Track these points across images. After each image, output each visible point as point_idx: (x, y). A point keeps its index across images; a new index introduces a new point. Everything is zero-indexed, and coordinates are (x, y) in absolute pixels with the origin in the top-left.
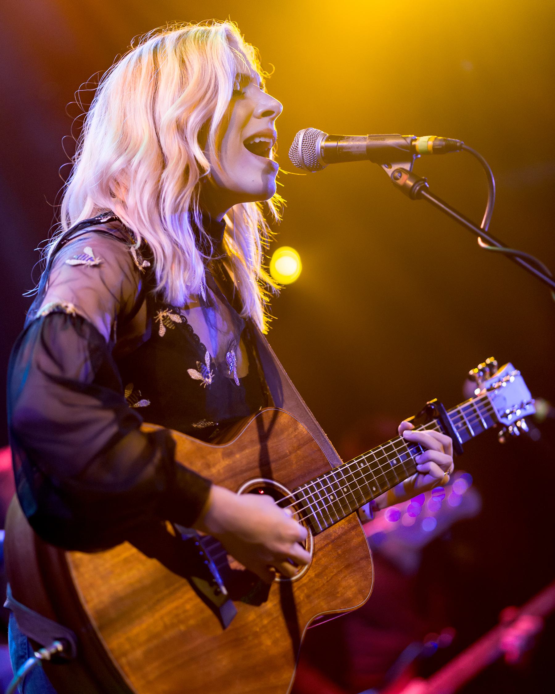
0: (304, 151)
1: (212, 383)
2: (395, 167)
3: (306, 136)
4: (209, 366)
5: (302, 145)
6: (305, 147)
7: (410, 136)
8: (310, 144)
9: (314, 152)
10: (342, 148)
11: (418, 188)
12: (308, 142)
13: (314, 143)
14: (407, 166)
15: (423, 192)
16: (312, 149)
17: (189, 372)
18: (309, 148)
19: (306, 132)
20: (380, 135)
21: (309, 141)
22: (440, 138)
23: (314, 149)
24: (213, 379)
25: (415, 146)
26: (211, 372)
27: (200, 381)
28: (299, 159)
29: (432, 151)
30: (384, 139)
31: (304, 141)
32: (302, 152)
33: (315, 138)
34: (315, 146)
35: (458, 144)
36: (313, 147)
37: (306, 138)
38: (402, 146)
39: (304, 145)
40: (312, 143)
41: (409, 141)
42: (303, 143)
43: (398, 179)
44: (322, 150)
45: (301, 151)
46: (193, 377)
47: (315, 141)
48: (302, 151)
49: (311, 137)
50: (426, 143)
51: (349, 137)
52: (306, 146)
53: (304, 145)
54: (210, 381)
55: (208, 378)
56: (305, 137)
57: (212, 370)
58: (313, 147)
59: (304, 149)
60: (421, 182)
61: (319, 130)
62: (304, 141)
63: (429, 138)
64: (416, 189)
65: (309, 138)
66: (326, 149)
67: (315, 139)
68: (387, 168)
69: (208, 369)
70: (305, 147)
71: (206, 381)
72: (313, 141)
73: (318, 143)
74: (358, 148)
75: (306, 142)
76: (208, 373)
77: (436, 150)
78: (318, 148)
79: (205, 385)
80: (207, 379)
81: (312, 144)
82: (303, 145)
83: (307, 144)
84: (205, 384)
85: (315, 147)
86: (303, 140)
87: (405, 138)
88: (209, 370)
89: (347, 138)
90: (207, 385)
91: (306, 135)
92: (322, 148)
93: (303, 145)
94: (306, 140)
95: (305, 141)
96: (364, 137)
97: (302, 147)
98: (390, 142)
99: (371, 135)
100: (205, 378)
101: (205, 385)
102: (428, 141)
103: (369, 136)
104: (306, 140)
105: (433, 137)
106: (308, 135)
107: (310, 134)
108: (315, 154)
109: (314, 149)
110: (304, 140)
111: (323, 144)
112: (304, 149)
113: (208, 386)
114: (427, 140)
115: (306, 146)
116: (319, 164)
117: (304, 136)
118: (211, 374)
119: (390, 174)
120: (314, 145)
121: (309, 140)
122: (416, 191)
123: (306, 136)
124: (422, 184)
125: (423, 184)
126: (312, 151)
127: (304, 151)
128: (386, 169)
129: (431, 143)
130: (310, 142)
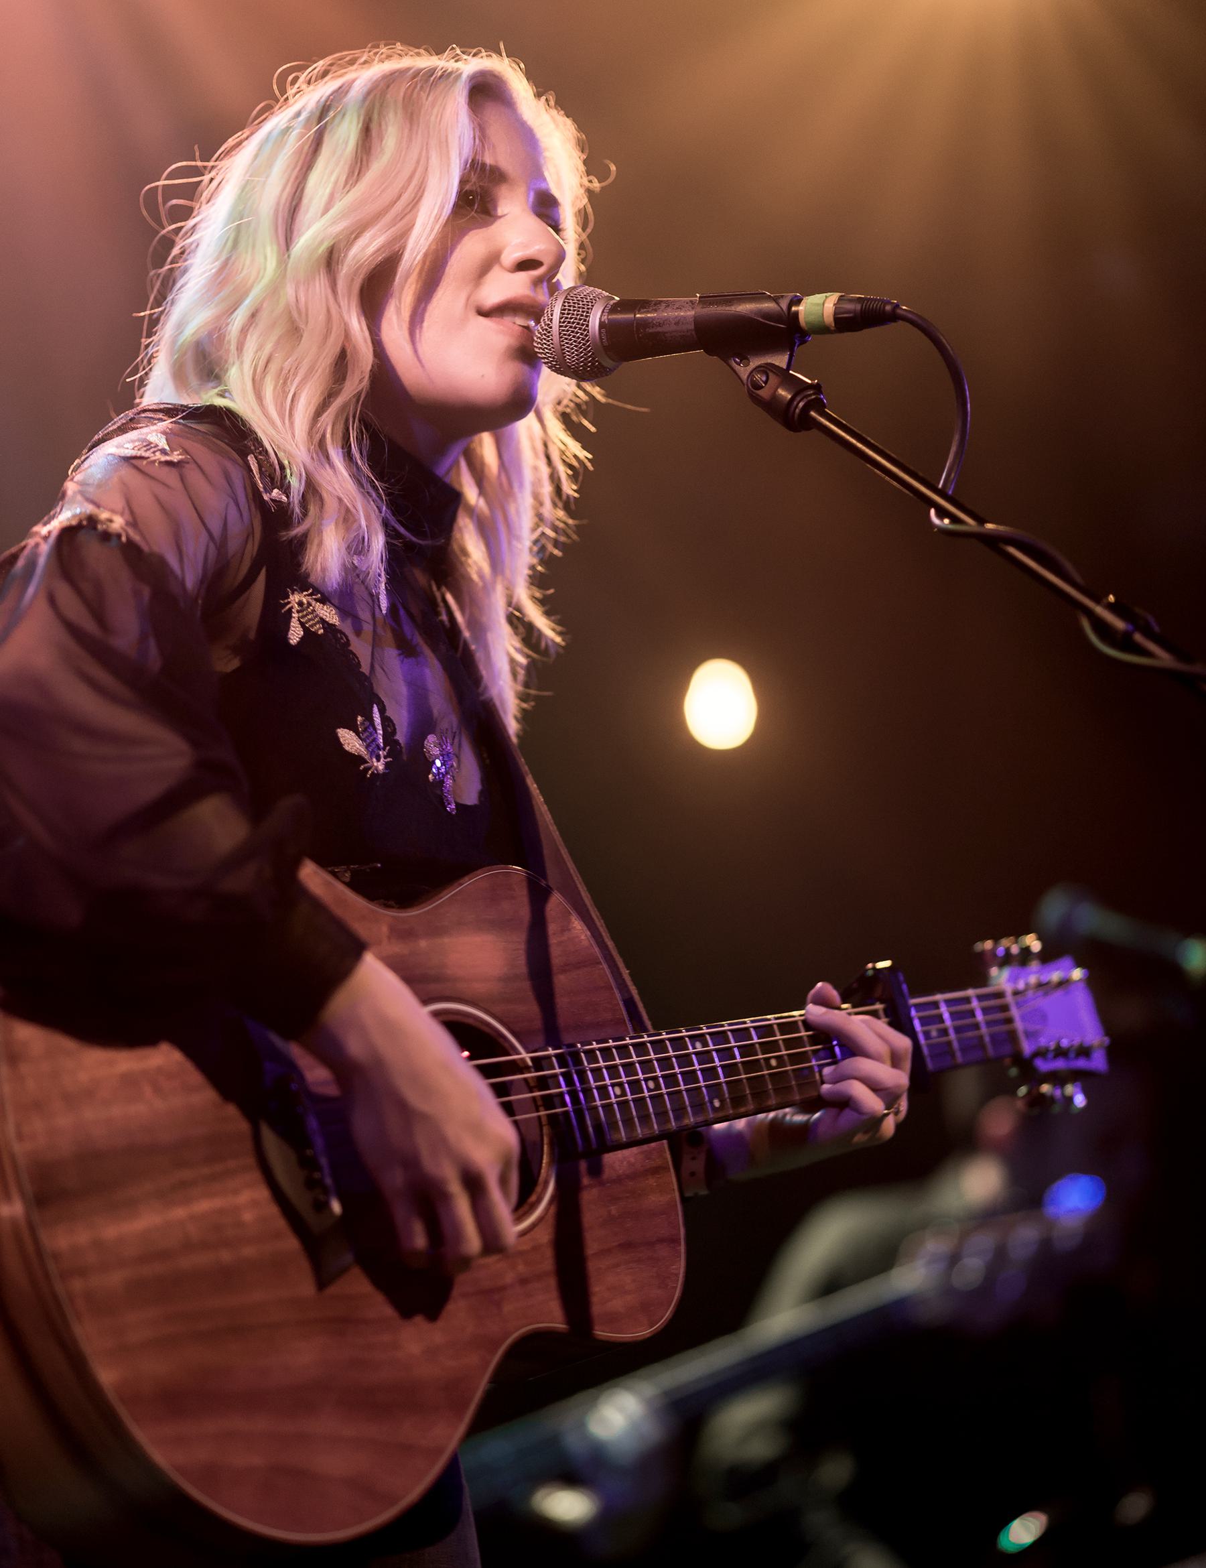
0: (565, 335)
3: (569, 303)
5: (560, 322)
8: (576, 319)
12: (573, 314)
13: (587, 316)
17: (339, 735)
18: (575, 328)
21: (575, 313)
23: (585, 330)
28: (553, 348)
31: (564, 314)
33: (588, 305)
34: (588, 322)
36: (583, 325)
37: (570, 306)
39: (564, 322)
40: (582, 315)
42: (561, 318)
46: (347, 748)
47: (588, 312)
48: (560, 334)
52: (569, 322)
53: (564, 322)
56: (566, 304)
58: (583, 325)
59: (563, 330)
62: (564, 314)
65: (574, 307)
67: (588, 309)
70: (566, 327)
75: (568, 314)
81: (580, 319)
82: (562, 320)
83: (571, 318)
86: (562, 310)
91: (569, 299)
93: (562, 320)
94: (570, 310)
95: (566, 312)
97: (560, 326)
104: (570, 310)
106: (573, 300)
107: (577, 298)
109: (585, 330)
110: (564, 310)
112: (563, 330)
115: (569, 322)
116: (597, 361)
121: (574, 311)
123: (569, 303)
126: (582, 334)
127: (565, 335)
130: (577, 315)
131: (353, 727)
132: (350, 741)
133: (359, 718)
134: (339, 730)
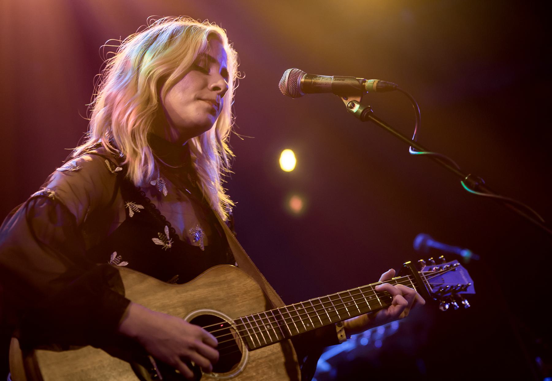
1: (172, 247)
2: (351, 99)
4: (168, 236)
6: (290, 82)
7: (361, 78)
9: (296, 85)
10: (315, 83)
11: (366, 113)
13: (297, 79)
14: (359, 99)
15: (369, 116)
16: (294, 83)
18: (293, 82)
19: (291, 71)
20: (342, 76)
22: (382, 81)
23: (296, 83)
24: (172, 244)
25: (364, 85)
26: (170, 240)
27: (162, 246)
29: (376, 90)
30: (344, 80)
32: (288, 85)
35: (394, 86)
38: (355, 86)
41: (361, 81)
42: (288, 79)
43: (352, 108)
44: (302, 84)
45: (287, 84)
48: (288, 84)
49: (294, 75)
50: (372, 84)
51: (321, 77)
53: (289, 80)
54: (170, 245)
55: (168, 244)
57: (171, 239)
60: (367, 110)
61: (300, 70)
63: (374, 81)
64: (364, 114)
66: (304, 84)
68: (345, 100)
69: (168, 238)
70: (290, 82)
71: (167, 246)
72: (296, 77)
73: (299, 79)
74: (325, 84)
75: (291, 78)
76: (168, 240)
77: (379, 89)
78: (299, 82)
79: (166, 249)
80: (167, 245)
81: (295, 80)
83: (292, 79)
84: (166, 247)
85: (297, 82)
87: (358, 80)
88: (169, 239)
89: (319, 78)
90: (167, 249)
92: (301, 83)
96: (331, 78)
97: (288, 82)
98: (348, 82)
99: (336, 76)
100: (165, 243)
101: (166, 249)
102: (373, 83)
103: (334, 77)
105: (377, 81)
108: (297, 87)
111: (303, 80)
113: (169, 249)
114: (373, 83)
117: (290, 74)
118: (171, 241)
119: (346, 105)
120: (296, 80)
121: (293, 77)
122: (365, 115)
124: (368, 110)
125: (369, 111)
126: (295, 85)
128: (344, 101)
129: (375, 84)
131: (157, 237)
132: (157, 241)
133: (159, 233)
134: (153, 239)
